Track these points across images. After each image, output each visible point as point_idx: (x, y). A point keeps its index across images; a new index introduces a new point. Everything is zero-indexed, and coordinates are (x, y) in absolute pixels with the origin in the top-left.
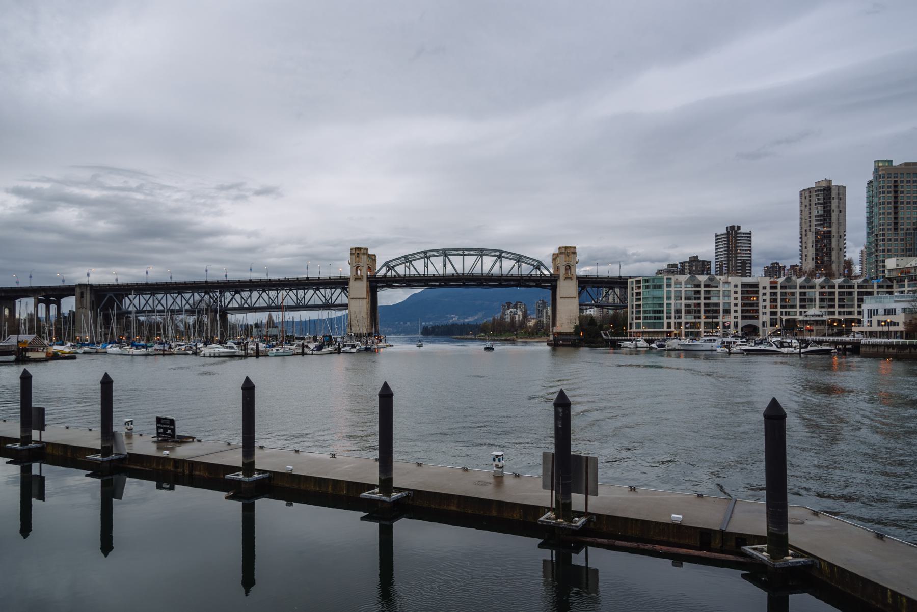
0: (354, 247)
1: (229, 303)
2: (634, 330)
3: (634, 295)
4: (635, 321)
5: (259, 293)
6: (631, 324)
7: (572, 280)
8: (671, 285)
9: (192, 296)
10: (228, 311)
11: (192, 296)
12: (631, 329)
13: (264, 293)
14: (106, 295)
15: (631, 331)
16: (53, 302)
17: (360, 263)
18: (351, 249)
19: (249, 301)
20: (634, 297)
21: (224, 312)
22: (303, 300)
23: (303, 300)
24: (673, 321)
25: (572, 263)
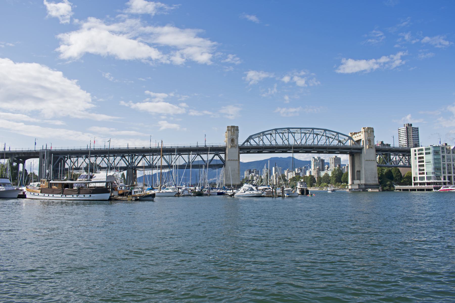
0: (230, 125)
1: (138, 163)
2: (418, 181)
3: (417, 158)
4: (418, 176)
5: (102, 158)
6: (414, 177)
7: (372, 149)
8: (444, 152)
9: (77, 161)
10: (137, 169)
11: (77, 161)
12: (414, 180)
13: (87, 159)
14: (59, 157)
15: (416, 182)
16: (21, 162)
17: (234, 136)
18: (228, 127)
19: (76, 164)
20: (417, 160)
21: (135, 169)
22: (113, 163)
23: (113, 163)
24: (447, 175)
25: (372, 138)
